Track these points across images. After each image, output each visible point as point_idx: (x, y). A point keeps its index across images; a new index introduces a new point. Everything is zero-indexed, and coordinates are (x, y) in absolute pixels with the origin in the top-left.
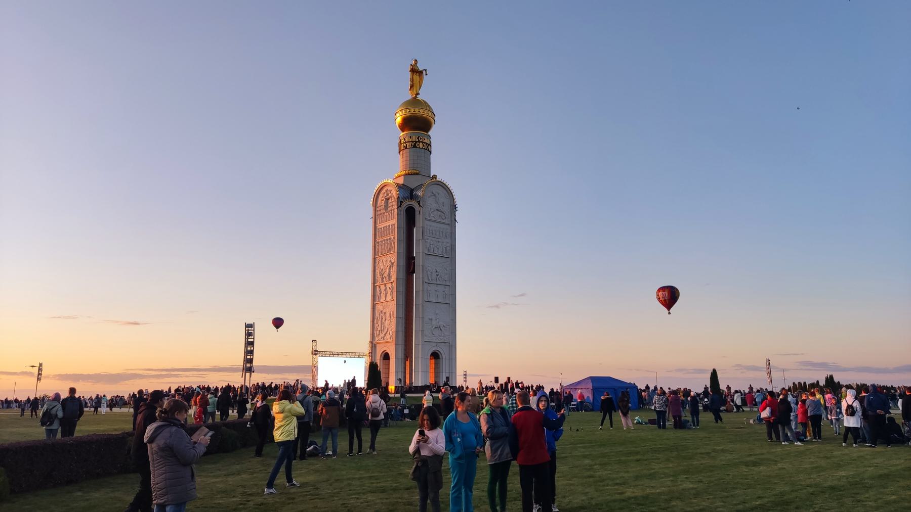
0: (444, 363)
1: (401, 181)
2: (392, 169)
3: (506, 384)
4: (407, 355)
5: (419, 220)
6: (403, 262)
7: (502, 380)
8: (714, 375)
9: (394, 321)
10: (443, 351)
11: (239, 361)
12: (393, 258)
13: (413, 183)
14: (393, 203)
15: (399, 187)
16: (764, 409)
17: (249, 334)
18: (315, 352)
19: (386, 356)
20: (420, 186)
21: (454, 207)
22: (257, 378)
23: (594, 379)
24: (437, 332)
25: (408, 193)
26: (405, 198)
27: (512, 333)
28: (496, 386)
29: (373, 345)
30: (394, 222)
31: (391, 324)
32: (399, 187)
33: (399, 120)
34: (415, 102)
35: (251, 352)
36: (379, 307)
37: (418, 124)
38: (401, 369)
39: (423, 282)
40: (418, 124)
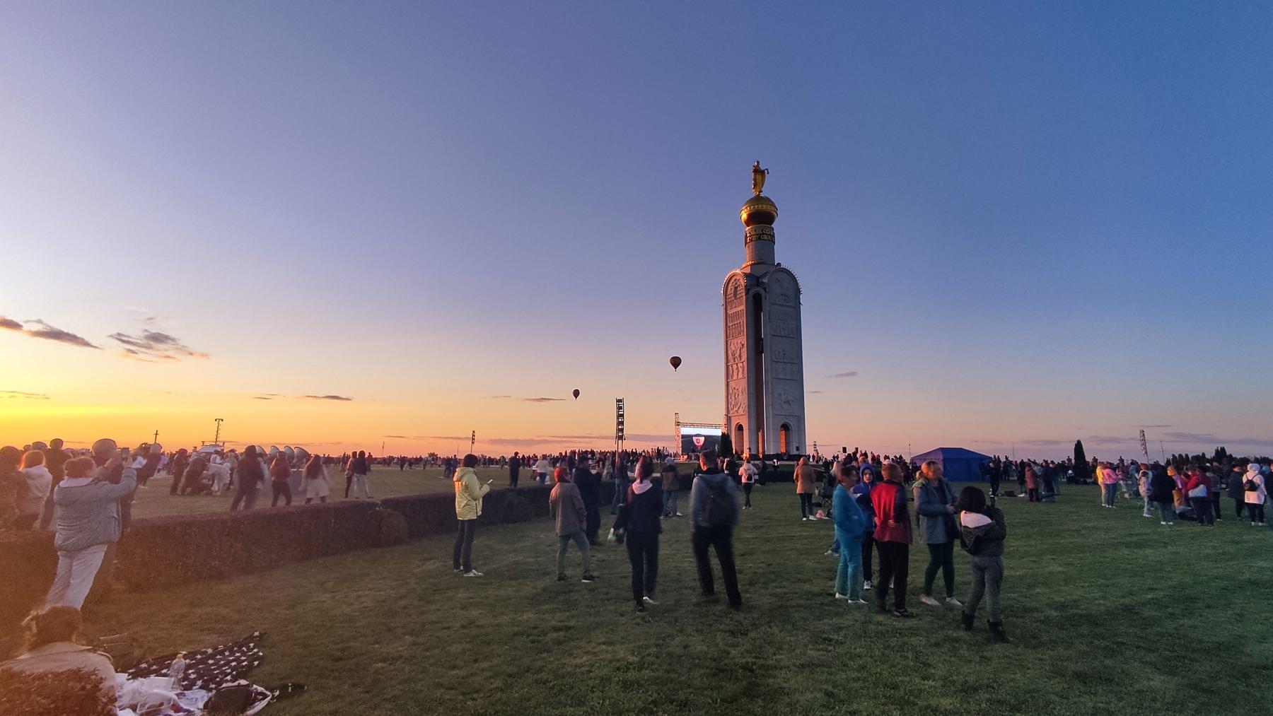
0: (794, 434)
1: (748, 271)
2: (740, 263)
3: (855, 453)
4: (759, 426)
5: (766, 305)
6: (752, 343)
7: (850, 451)
8: (1079, 446)
9: (746, 396)
10: (792, 423)
11: (613, 431)
12: (743, 339)
13: (760, 271)
14: (742, 290)
15: (746, 275)
16: (1196, 486)
17: (619, 408)
18: (678, 424)
19: (740, 428)
20: (764, 275)
21: (798, 292)
22: (628, 446)
23: (941, 449)
24: (786, 406)
25: (754, 280)
26: (752, 286)
27: (860, 404)
28: (842, 457)
29: (729, 419)
30: (743, 307)
31: (743, 399)
32: (746, 275)
33: (744, 216)
34: (758, 199)
35: (622, 423)
36: (732, 384)
37: (762, 218)
38: (754, 439)
39: (772, 361)
40: (762, 218)
